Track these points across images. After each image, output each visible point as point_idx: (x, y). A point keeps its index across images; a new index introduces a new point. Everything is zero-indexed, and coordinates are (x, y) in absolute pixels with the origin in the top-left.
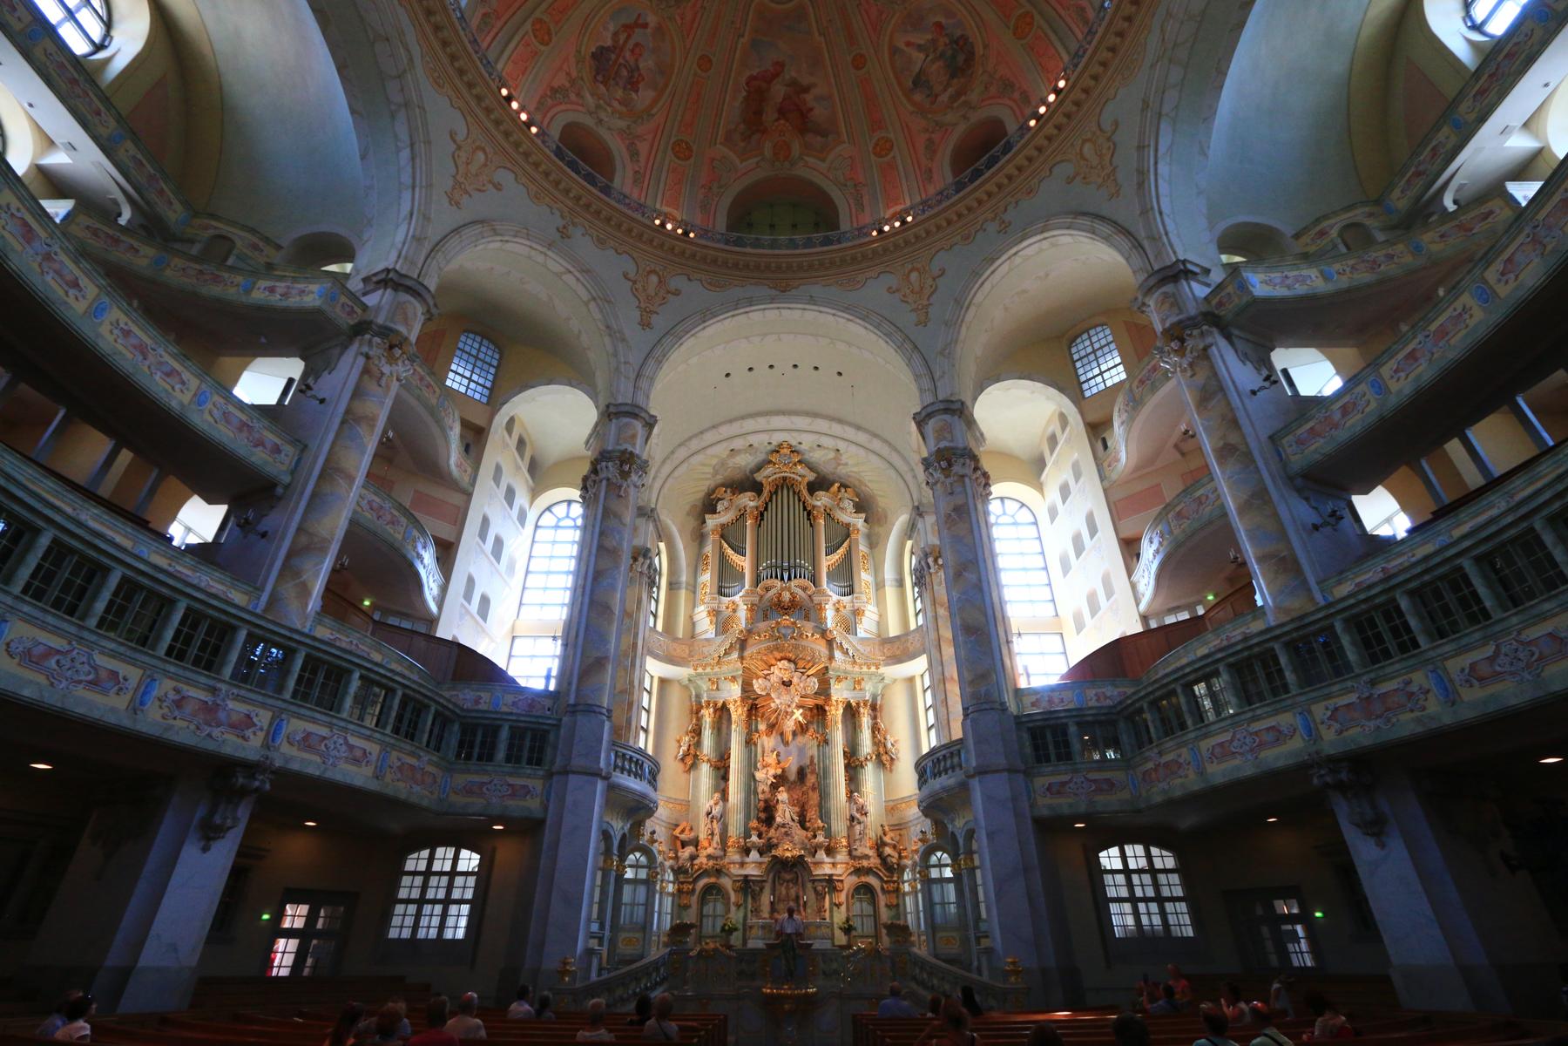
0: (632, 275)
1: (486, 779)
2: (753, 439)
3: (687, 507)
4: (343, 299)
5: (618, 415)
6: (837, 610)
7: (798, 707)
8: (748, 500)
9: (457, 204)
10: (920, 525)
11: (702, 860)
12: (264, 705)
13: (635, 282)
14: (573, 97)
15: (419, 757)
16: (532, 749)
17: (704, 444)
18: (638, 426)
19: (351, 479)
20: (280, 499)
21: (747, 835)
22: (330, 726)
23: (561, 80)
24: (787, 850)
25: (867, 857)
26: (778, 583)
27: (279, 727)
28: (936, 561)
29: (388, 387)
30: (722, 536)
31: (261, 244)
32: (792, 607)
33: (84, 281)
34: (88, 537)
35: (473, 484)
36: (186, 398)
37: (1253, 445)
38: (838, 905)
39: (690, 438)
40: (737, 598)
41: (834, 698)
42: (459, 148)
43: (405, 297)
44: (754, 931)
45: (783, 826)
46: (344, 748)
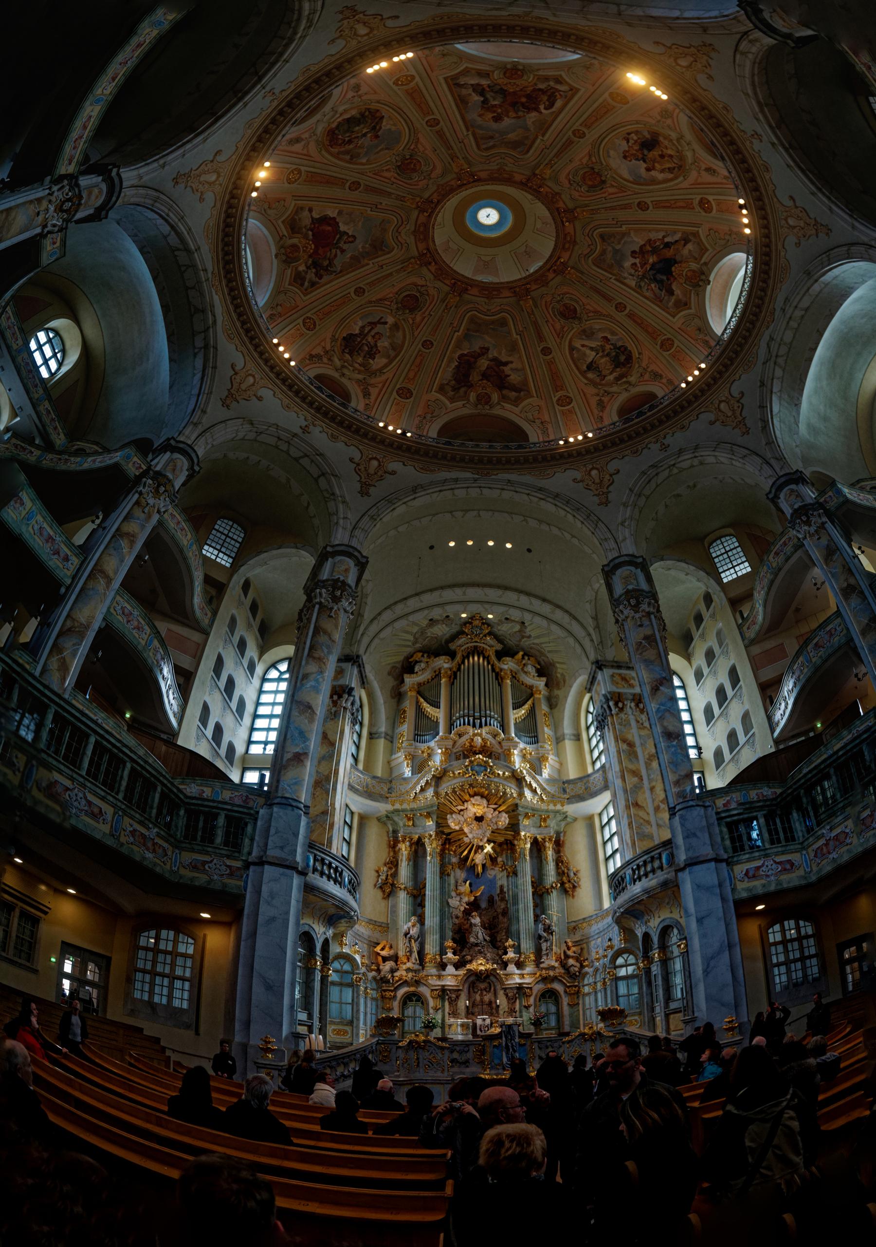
3: (389, 667)
6: (524, 757)
7: (489, 841)
10: (599, 677)
11: (401, 973)
21: (443, 952)
24: (480, 965)
25: (553, 968)
26: (471, 730)
28: (616, 704)
30: (419, 693)
32: (485, 750)
38: (527, 1007)
39: (396, 603)
40: (432, 744)
41: (523, 833)
44: (453, 1028)
45: (477, 945)
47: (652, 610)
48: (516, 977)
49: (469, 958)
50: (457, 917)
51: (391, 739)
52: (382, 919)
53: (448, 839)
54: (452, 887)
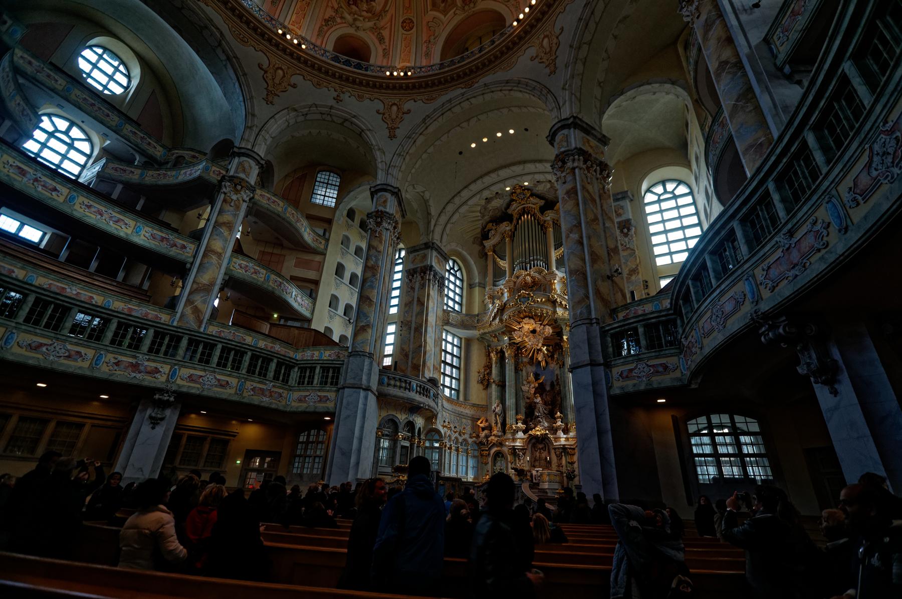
0: (381, 111)
1: (307, 394)
2: (495, 189)
4: (214, 168)
5: (377, 192)
7: (543, 345)
8: (505, 227)
9: (271, 103)
12: (164, 363)
13: (384, 114)
14: (339, 20)
15: (266, 384)
16: (333, 377)
17: (463, 200)
18: (388, 195)
19: (219, 255)
20: (190, 269)
22: (205, 370)
23: (330, 13)
24: (538, 431)
26: (524, 273)
27: (175, 373)
29: (238, 208)
30: (494, 251)
31: (197, 155)
33: (59, 187)
34: (52, 295)
35: (326, 249)
36: (129, 231)
37: (744, 50)
38: (572, 463)
42: (266, 72)
43: (243, 159)
45: (538, 417)
46: (214, 380)
47: (576, 164)
48: (563, 439)
49: (533, 426)
50: (528, 398)
51: (482, 286)
52: (484, 403)
53: (518, 348)
54: (524, 377)
